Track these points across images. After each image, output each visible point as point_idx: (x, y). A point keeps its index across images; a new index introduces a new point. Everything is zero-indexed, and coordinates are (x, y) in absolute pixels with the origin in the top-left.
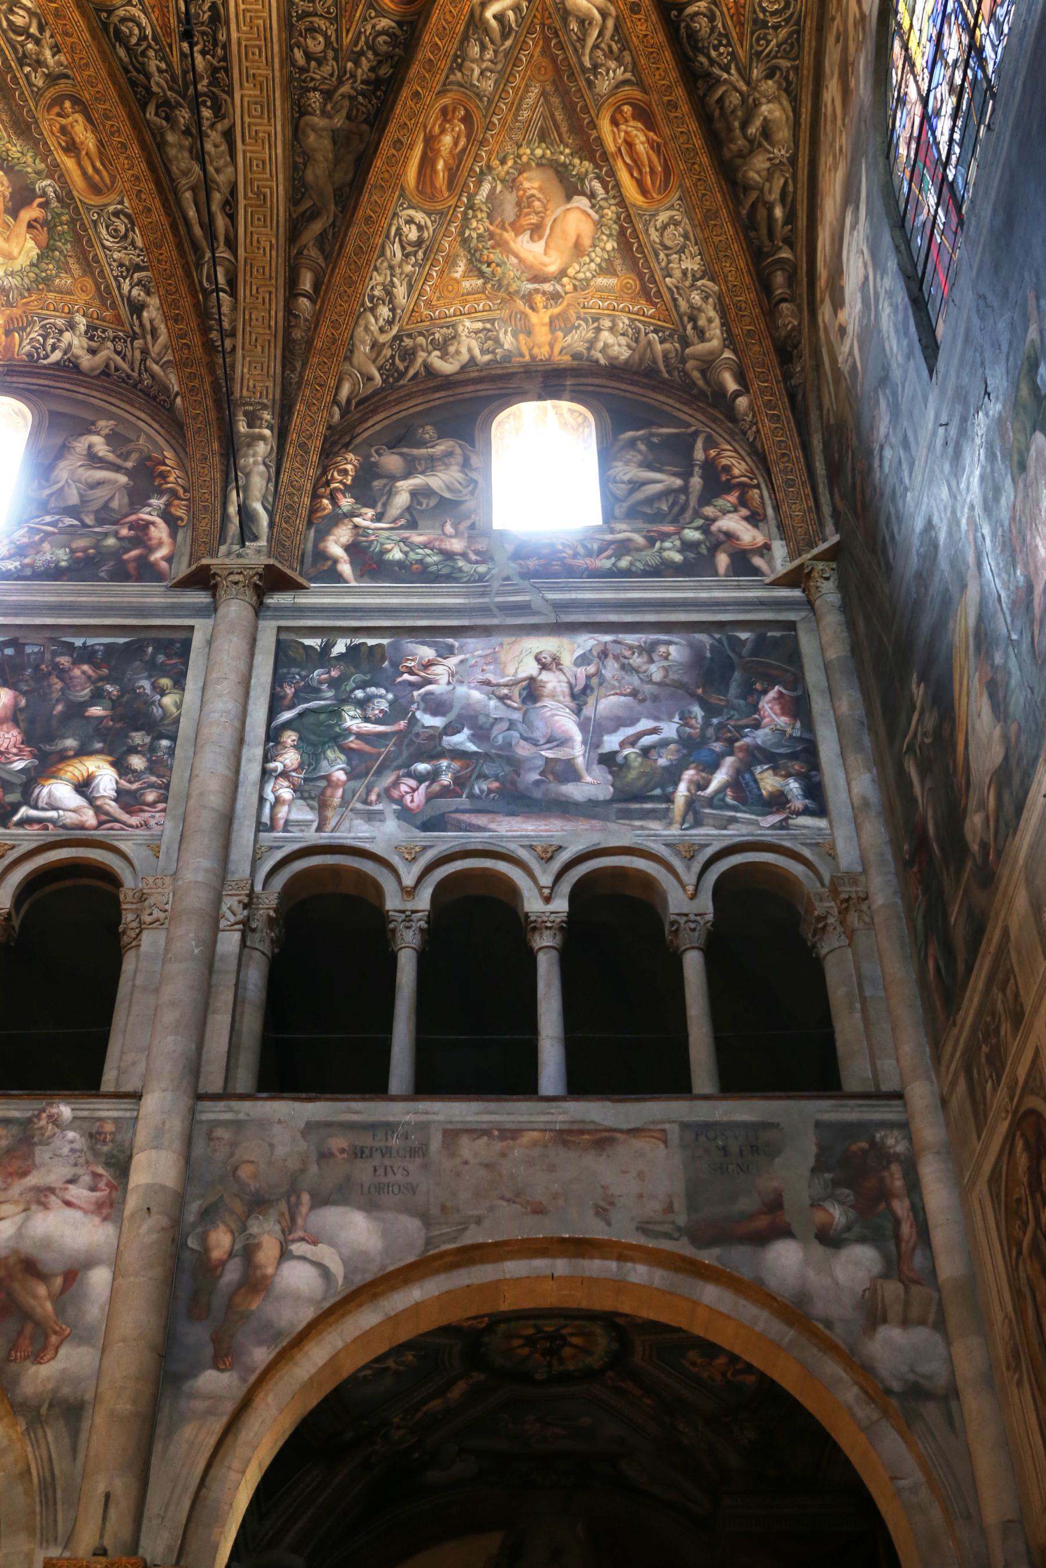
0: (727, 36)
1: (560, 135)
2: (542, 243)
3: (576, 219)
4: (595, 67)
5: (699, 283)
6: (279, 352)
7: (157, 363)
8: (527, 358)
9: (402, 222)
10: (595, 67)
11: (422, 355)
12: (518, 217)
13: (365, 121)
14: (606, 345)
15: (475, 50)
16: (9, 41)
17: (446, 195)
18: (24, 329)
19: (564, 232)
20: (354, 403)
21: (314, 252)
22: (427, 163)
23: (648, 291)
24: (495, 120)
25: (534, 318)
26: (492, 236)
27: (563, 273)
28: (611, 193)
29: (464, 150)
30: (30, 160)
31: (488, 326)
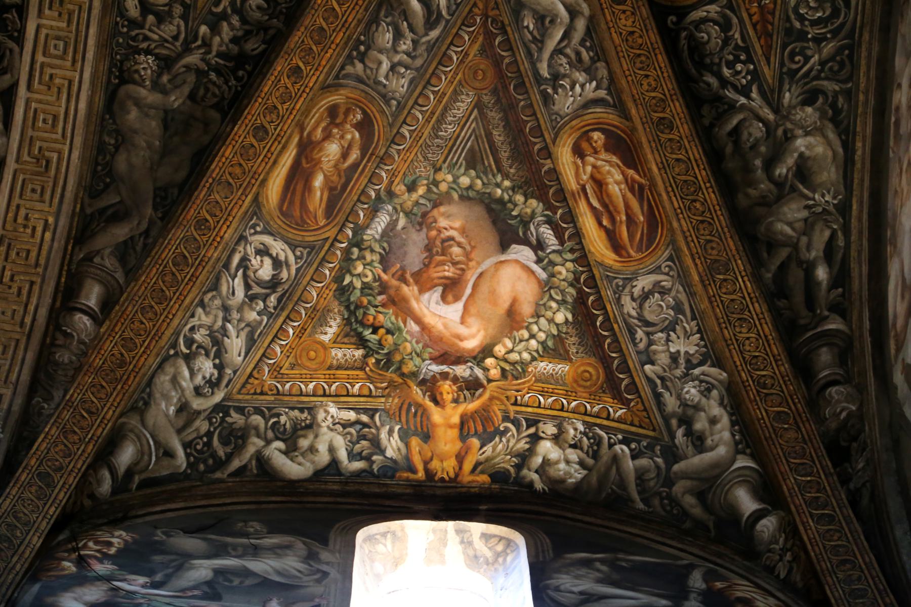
0: (747, 50)
1: (497, 162)
2: (459, 306)
3: (514, 277)
4: (556, 77)
5: (697, 371)
6: (30, 356)
8: (421, 474)
9: (250, 250)
10: (556, 77)
11: (255, 443)
12: (426, 266)
13: (216, 107)
14: (546, 462)
15: (386, 37)
17: (322, 222)
19: (493, 292)
20: (137, 479)
21: (110, 263)
22: (299, 175)
23: (614, 381)
24: (405, 131)
25: (436, 415)
26: (384, 288)
27: (486, 351)
28: (568, 245)
29: (355, 166)
31: (365, 418)
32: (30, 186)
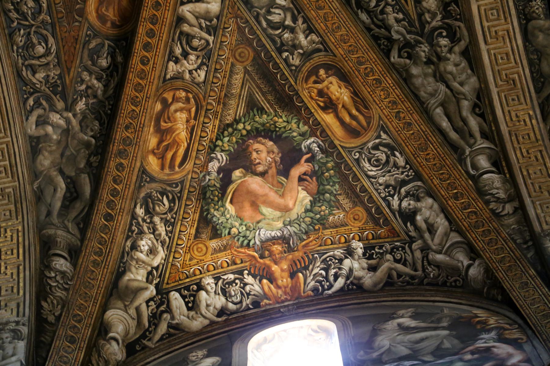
7: (440, 253)
16: (270, 37)
18: (306, 268)
30: (294, 126)
32: (510, 98)
